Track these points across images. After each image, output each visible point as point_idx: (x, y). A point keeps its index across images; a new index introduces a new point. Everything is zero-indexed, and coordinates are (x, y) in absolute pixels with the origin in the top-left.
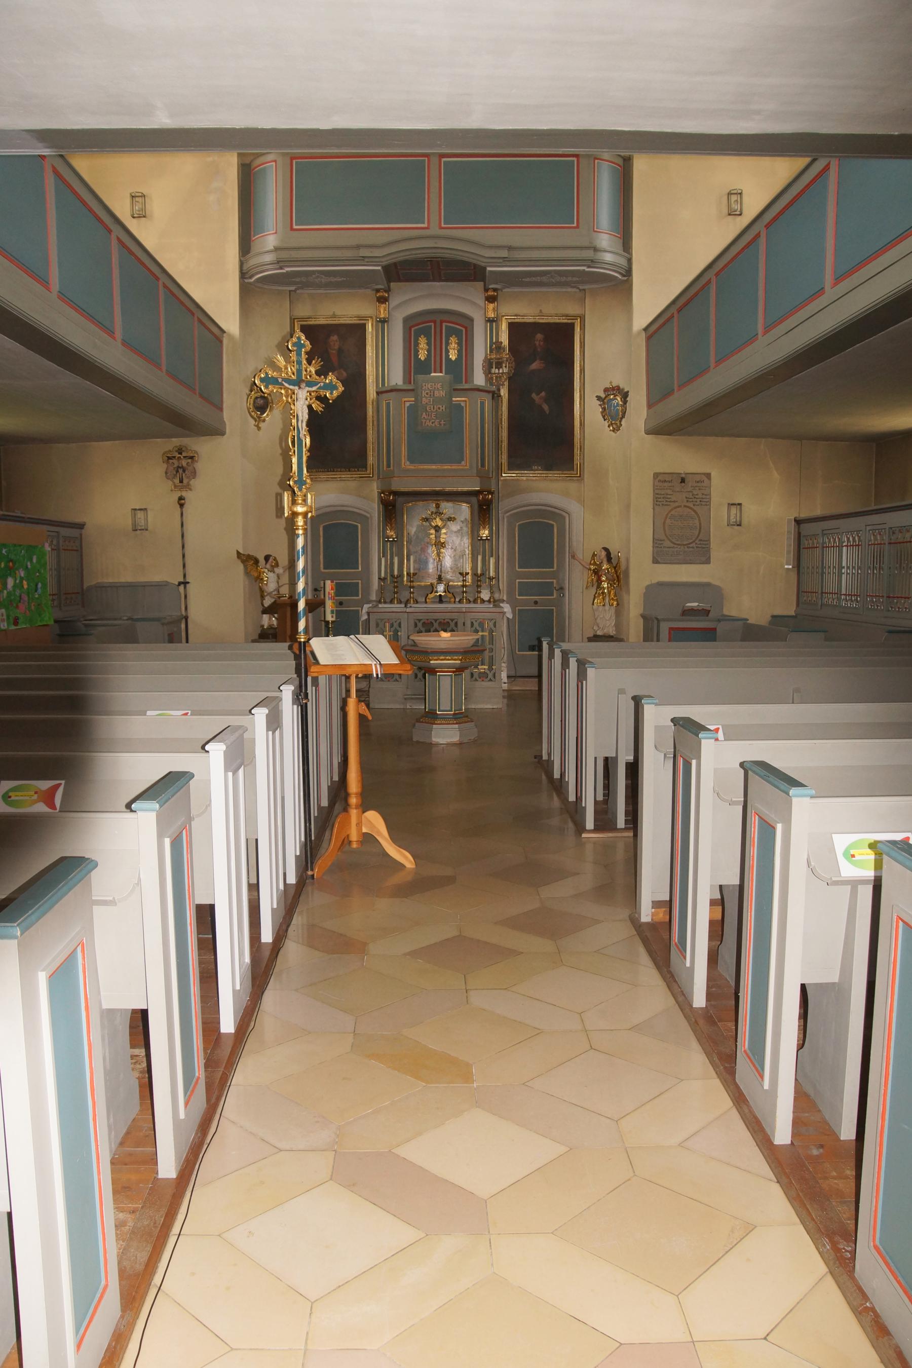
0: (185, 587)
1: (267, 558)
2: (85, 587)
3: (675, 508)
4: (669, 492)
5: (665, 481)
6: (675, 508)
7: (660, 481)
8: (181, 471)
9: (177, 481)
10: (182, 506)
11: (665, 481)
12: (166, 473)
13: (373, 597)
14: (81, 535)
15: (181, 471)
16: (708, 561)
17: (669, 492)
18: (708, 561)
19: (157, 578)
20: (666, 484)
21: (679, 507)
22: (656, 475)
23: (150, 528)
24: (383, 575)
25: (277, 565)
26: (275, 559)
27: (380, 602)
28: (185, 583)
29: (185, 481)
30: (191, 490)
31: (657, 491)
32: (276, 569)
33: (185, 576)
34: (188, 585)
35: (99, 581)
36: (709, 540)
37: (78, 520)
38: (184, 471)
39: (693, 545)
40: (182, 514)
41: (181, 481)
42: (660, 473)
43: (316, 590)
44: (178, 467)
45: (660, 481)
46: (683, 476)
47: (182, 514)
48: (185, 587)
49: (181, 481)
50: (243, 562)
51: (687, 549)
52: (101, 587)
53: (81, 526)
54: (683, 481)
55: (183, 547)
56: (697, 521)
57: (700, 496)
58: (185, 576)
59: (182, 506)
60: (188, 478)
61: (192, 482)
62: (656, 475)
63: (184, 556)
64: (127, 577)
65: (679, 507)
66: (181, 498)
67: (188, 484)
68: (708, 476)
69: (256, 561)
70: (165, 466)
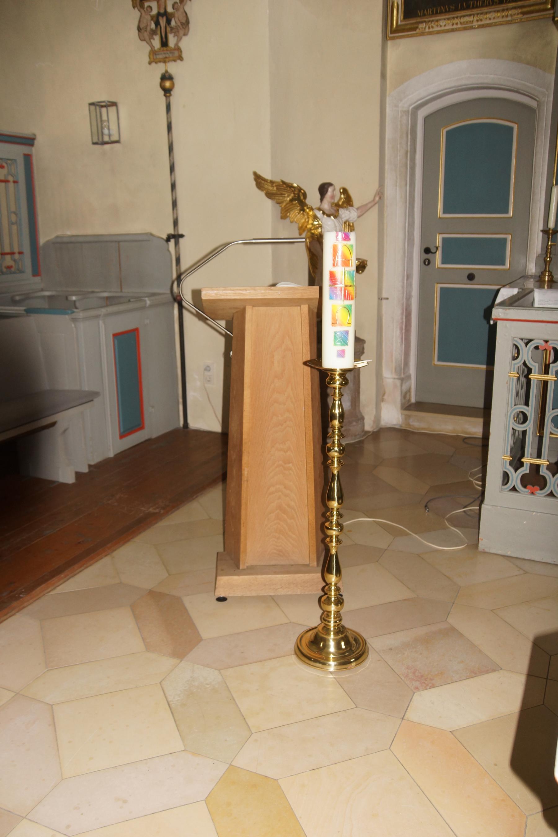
0: (177, 244)
1: (323, 189)
2: (42, 240)
8: (163, 21)
9: (156, 42)
10: (167, 92)
12: (139, 29)
13: (532, 268)
14: (28, 158)
15: (163, 21)
19: (135, 226)
23: (124, 137)
24: (552, 224)
25: (348, 201)
26: (345, 191)
27: (540, 282)
28: (176, 237)
29: (172, 41)
30: (181, 58)
32: (342, 212)
33: (176, 223)
34: (181, 240)
35: (59, 233)
37: (25, 131)
38: (168, 22)
40: (168, 108)
41: (164, 43)
43: (427, 251)
44: (159, 14)
47: (168, 108)
48: (177, 244)
49: (164, 43)
50: (269, 195)
52: (61, 244)
53: (29, 141)
55: (172, 169)
58: (176, 223)
59: (167, 92)
60: (176, 34)
61: (182, 45)
63: (173, 186)
64: (96, 227)
66: (166, 77)
67: (179, 49)
69: (299, 198)
70: (136, 14)
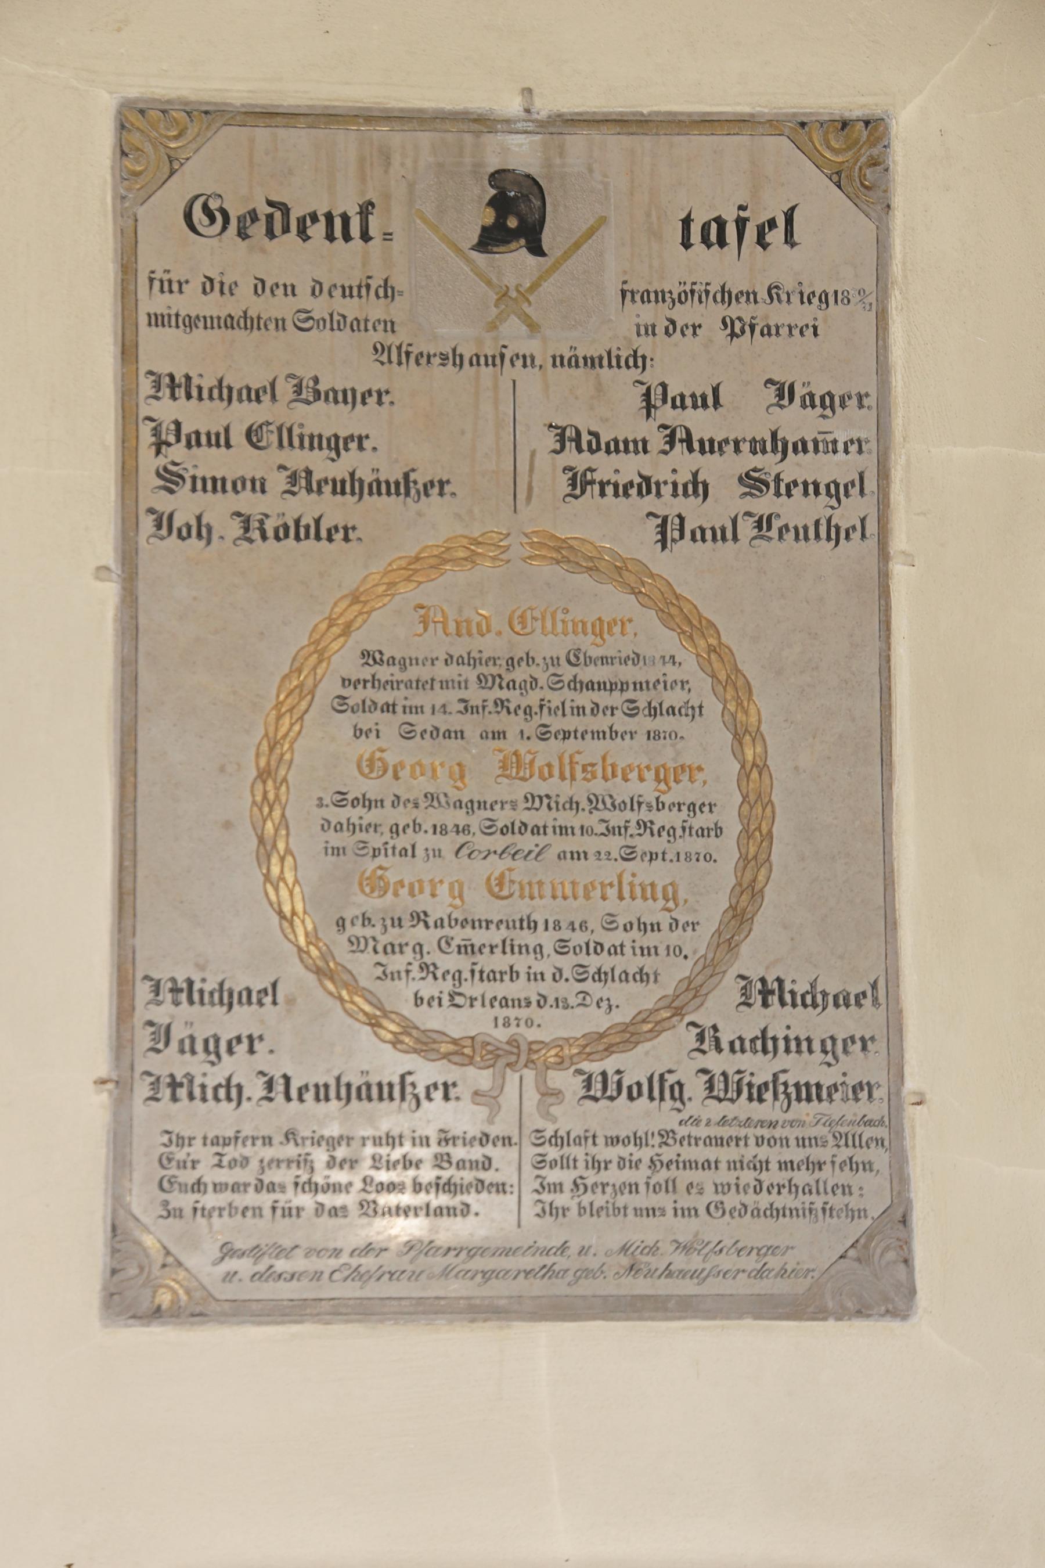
3: (419, 567)
4: (340, 359)
5: (278, 219)
6: (419, 567)
7: (204, 214)
11: (278, 219)
16: (873, 1277)
17: (340, 359)
18: (873, 1277)
20: (289, 259)
21: (472, 552)
22: (152, 135)
31: (164, 351)
36: (881, 992)
39: (669, 1052)
42: (209, 116)
45: (204, 214)
46: (521, 153)
51: (573, 1116)
54: (515, 215)
56: (707, 742)
57: (750, 415)
62: (152, 135)
65: (472, 552)
68: (853, 151)
